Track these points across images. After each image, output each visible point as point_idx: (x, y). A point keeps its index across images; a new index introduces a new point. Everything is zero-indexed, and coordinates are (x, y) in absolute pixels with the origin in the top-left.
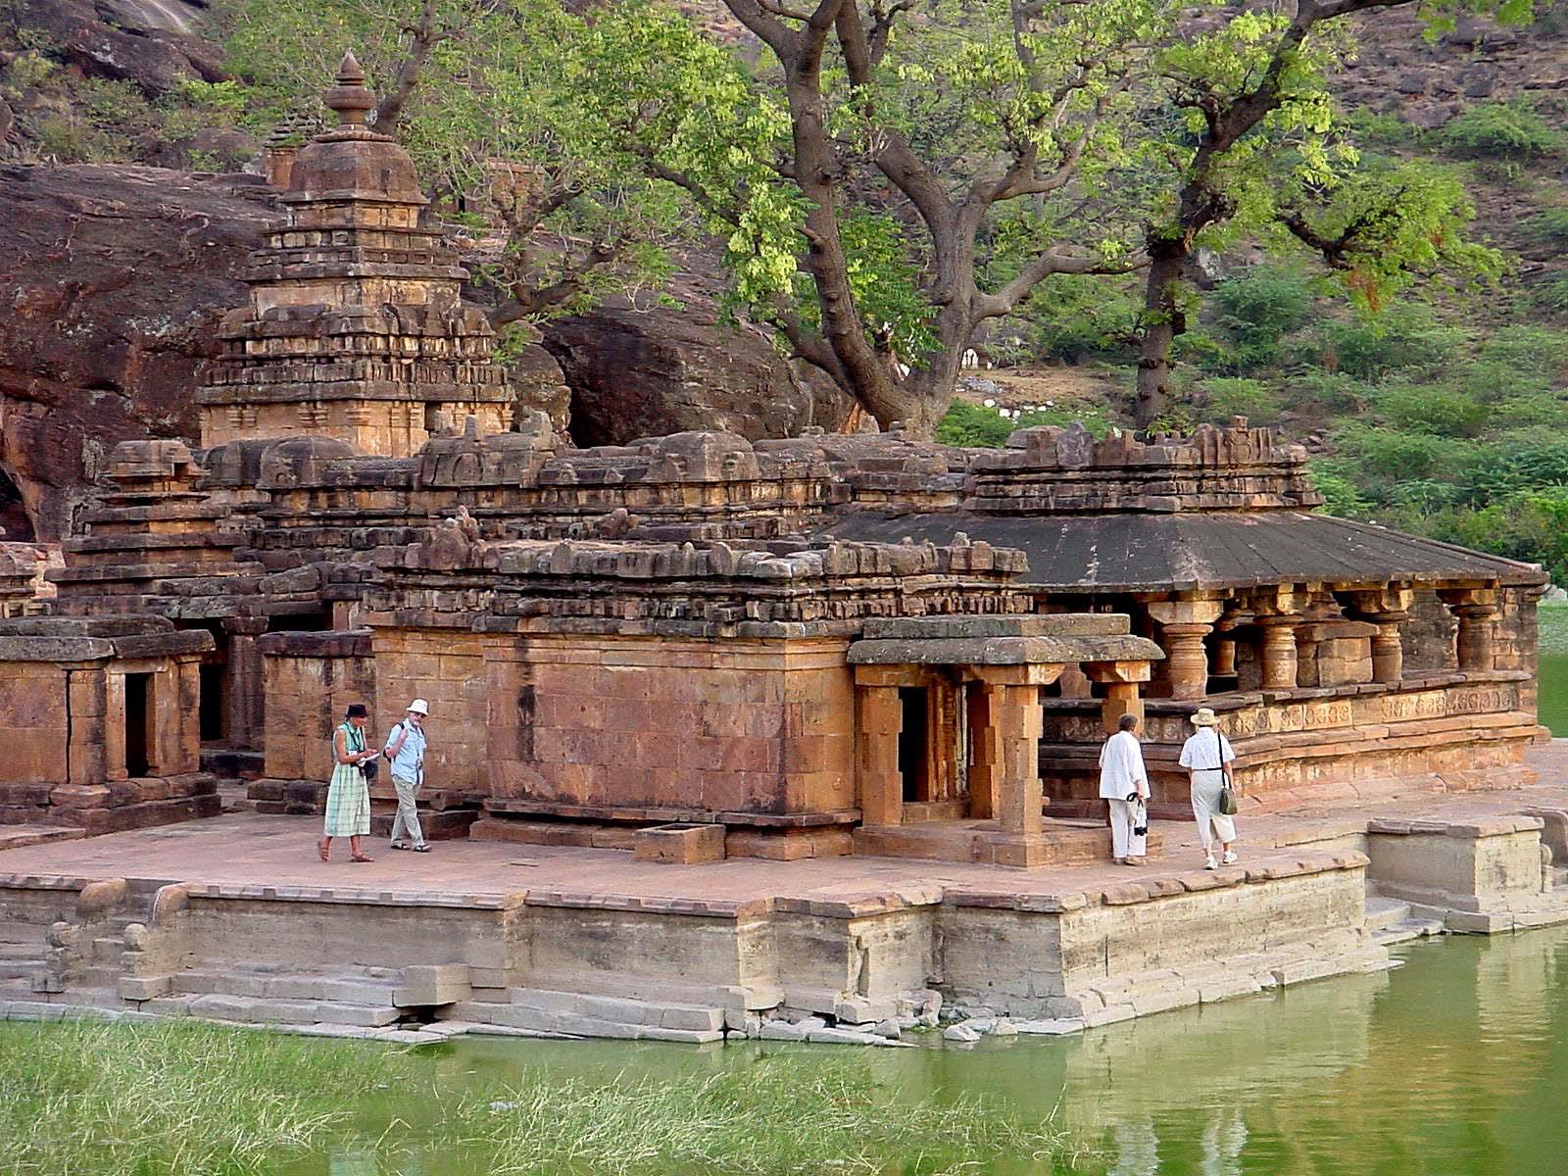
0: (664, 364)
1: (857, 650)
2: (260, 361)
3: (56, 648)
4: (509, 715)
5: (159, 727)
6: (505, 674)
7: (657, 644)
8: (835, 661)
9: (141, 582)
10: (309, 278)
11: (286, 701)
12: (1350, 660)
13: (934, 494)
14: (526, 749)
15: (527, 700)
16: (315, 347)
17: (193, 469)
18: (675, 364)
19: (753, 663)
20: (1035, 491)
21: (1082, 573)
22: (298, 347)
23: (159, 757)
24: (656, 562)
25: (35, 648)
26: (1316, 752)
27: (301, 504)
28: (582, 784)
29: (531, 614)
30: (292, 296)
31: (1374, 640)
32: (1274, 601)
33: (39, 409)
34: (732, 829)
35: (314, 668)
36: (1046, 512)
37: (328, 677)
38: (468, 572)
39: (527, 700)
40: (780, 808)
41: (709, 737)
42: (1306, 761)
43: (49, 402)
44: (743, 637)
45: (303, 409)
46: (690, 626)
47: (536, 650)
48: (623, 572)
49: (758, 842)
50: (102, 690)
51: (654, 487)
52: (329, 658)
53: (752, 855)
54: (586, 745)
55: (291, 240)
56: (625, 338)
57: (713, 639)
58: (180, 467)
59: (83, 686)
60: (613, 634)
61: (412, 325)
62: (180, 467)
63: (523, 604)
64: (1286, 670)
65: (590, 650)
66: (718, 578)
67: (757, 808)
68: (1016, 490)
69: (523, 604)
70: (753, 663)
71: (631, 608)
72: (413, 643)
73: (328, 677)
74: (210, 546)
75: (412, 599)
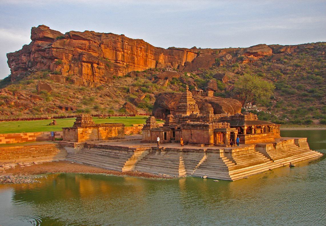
0: (221, 108)
1: (215, 131)
2: (180, 108)
3: (159, 130)
4: (190, 136)
5: (167, 136)
6: (190, 132)
7: (200, 130)
8: (213, 132)
9: (169, 125)
10: (184, 102)
11: (177, 134)
12: (258, 131)
13: (228, 118)
14: (191, 138)
15: (191, 134)
16: (184, 107)
17: (173, 117)
18: (222, 107)
19: (207, 132)
20: (235, 118)
21: (237, 125)
22: (183, 107)
23: (167, 138)
24: (200, 124)
25: (158, 130)
26: (255, 139)
27: (181, 119)
28: (195, 141)
29: (192, 128)
30: (182, 103)
31: (261, 130)
32: (252, 127)
33: (173, 111)
34: (205, 144)
35: (178, 132)
36: (235, 120)
37: (179, 133)
38: (188, 125)
39: (191, 134)
40: (209, 143)
41: (204, 137)
42: (254, 139)
43: (174, 111)
44: (206, 130)
45: (183, 112)
46: (202, 129)
47: (192, 131)
48: (198, 125)
49: (207, 145)
50: (162, 134)
51: (206, 118)
52: (179, 131)
53: (206, 146)
54: (195, 138)
55: (182, 99)
56: (218, 105)
57: (204, 130)
58: (172, 117)
59: (161, 133)
60: (197, 130)
61: (191, 106)
62: (172, 117)
63: (191, 127)
64: (253, 132)
65: (195, 131)
66: (204, 125)
67: (207, 143)
68: (234, 118)
69: (191, 127)
70: (207, 132)
71: (198, 128)
72: (184, 130)
73: (179, 133)
74: (174, 123)
75: (184, 127)
